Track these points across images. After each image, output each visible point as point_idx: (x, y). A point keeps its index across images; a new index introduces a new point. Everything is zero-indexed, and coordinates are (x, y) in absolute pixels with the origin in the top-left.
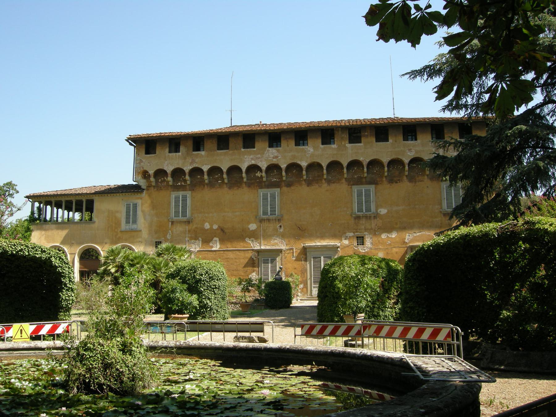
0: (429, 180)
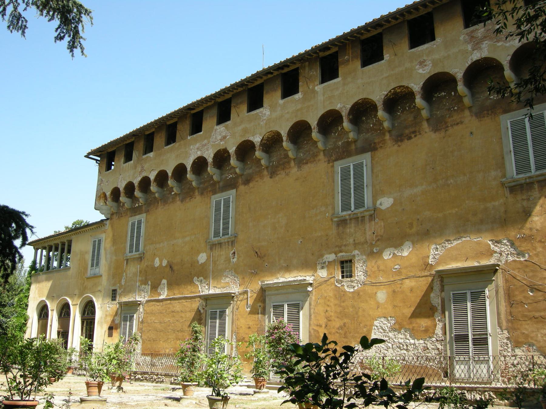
0: (474, 118)
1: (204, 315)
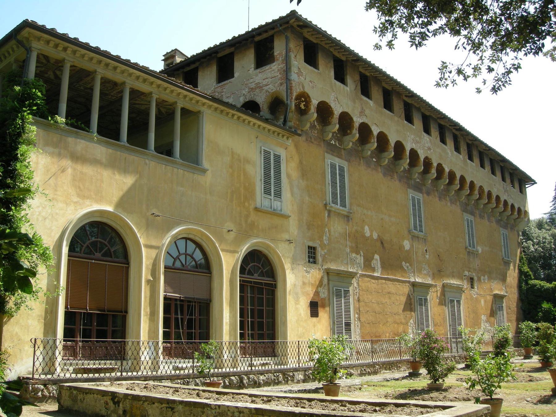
1: (413, 300)
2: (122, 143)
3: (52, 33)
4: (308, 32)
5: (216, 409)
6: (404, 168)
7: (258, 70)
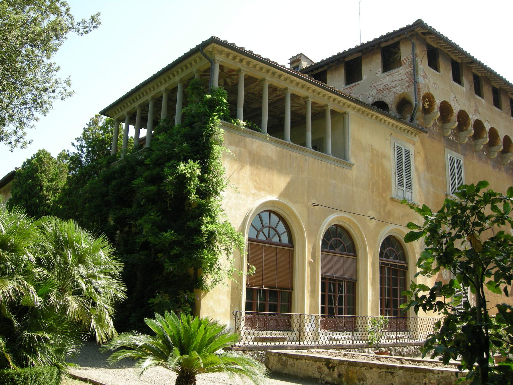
2: (288, 142)
3: (232, 47)
4: (430, 38)
5: (438, 373)
6: (511, 161)
7: (386, 74)
